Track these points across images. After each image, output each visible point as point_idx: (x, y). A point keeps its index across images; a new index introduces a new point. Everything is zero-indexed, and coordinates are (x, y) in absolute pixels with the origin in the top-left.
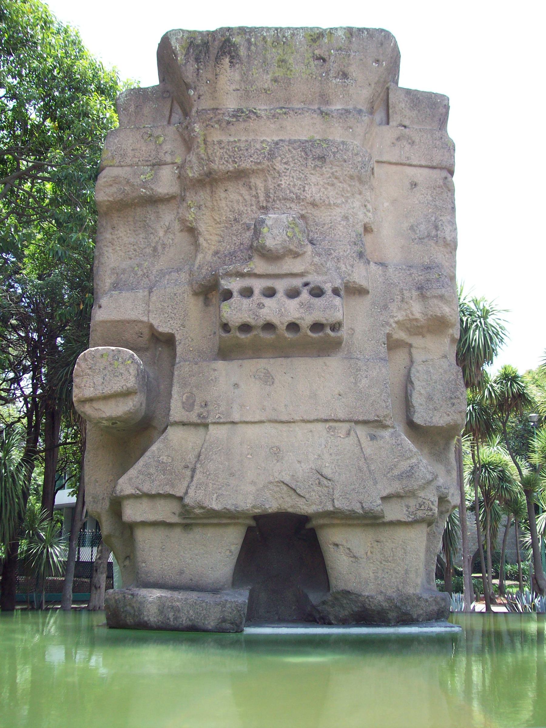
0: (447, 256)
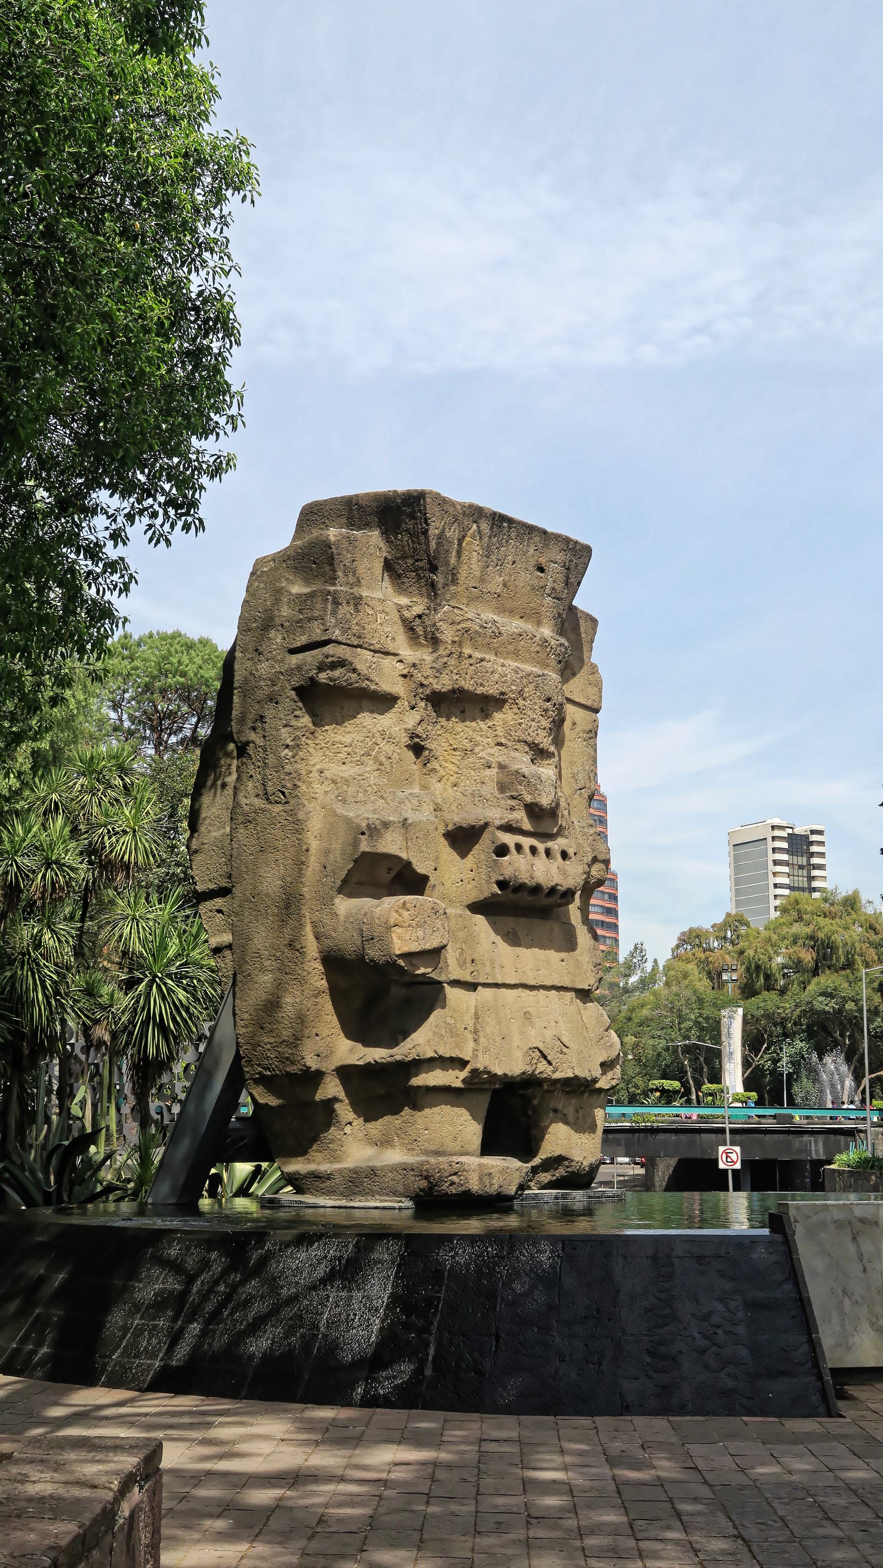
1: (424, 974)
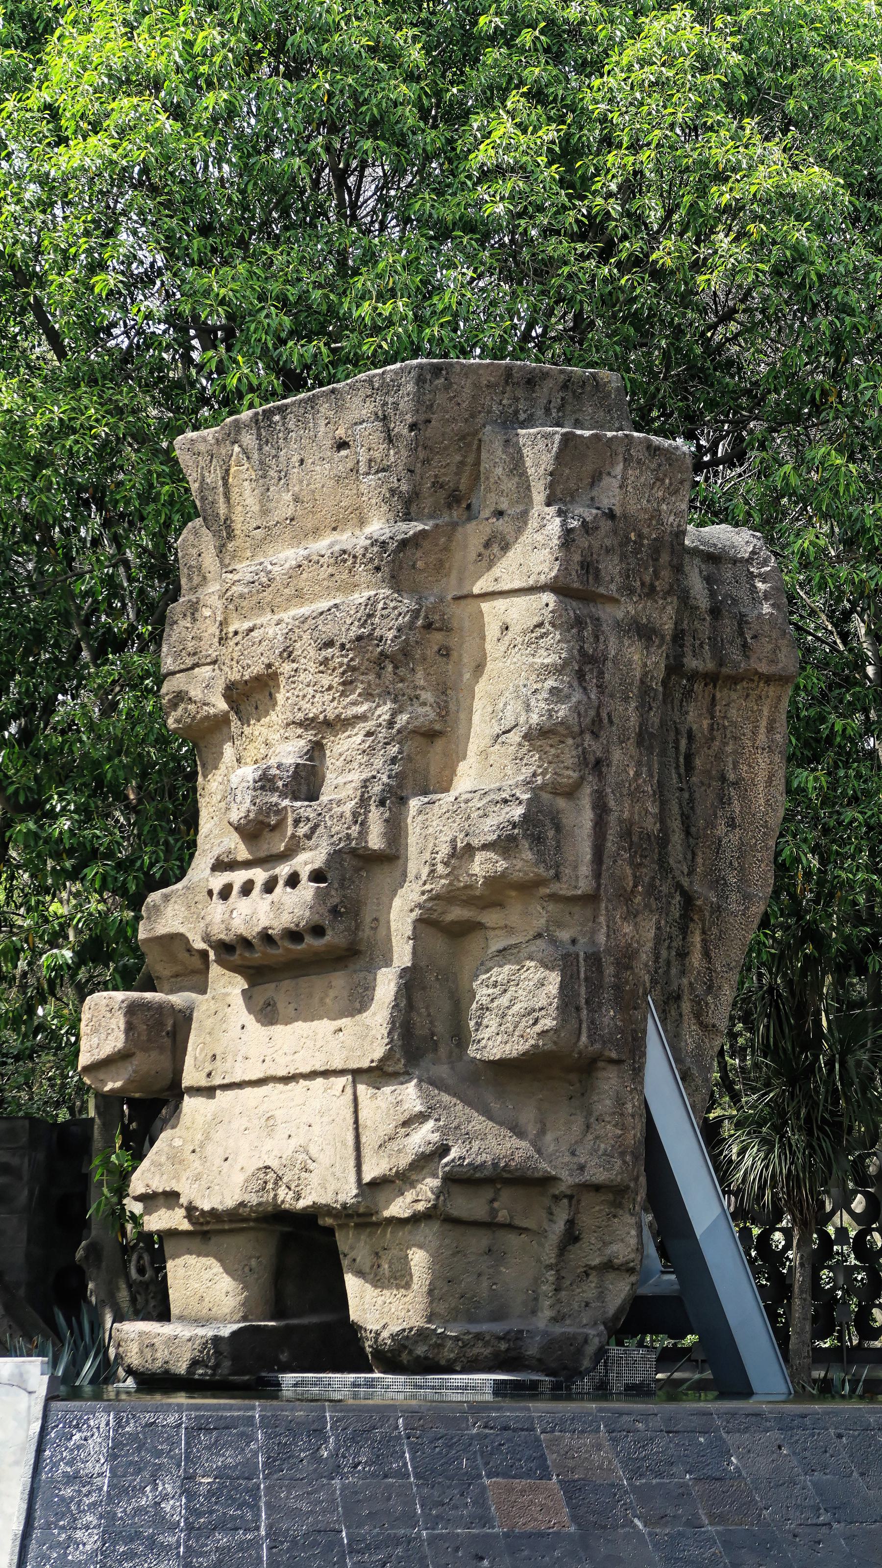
0: (553, 751)
1: (111, 1090)
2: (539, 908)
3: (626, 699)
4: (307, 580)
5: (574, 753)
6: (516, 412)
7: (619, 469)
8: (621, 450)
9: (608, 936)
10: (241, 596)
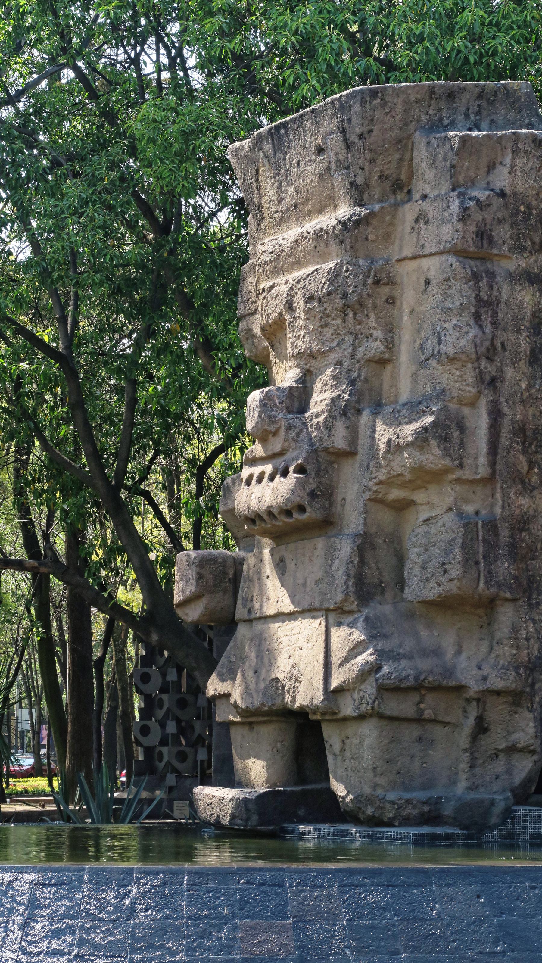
0: (458, 373)
2: (449, 489)
3: (518, 331)
4: (301, 251)
5: (473, 374)
6: (441, 119)
7: (508, 159)
8: (509, 145)
9: (503, 507)
10: (265, 263)
